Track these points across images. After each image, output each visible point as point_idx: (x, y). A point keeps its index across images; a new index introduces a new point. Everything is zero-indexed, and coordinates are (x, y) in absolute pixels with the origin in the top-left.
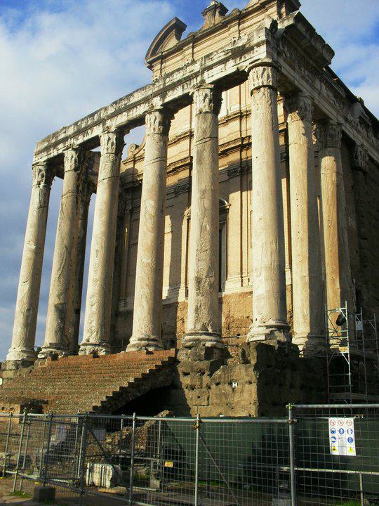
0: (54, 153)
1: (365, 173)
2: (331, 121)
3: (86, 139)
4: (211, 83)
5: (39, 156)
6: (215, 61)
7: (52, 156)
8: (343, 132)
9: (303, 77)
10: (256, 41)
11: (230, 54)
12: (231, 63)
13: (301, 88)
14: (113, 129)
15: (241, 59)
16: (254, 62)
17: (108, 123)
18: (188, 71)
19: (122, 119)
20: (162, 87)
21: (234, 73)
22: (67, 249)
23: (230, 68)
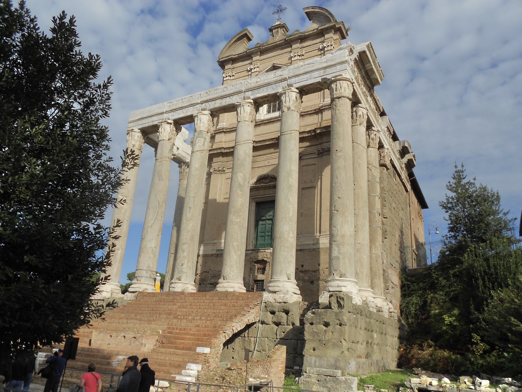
1: (388, 169)
2: (373, 128)
5: (134, 124)
8: (379, 138)
9: (364, 93)
13: (361, 100)
14: (207, 112)
16: (336, 76)
21: (319, 83)
22: (159, 203)
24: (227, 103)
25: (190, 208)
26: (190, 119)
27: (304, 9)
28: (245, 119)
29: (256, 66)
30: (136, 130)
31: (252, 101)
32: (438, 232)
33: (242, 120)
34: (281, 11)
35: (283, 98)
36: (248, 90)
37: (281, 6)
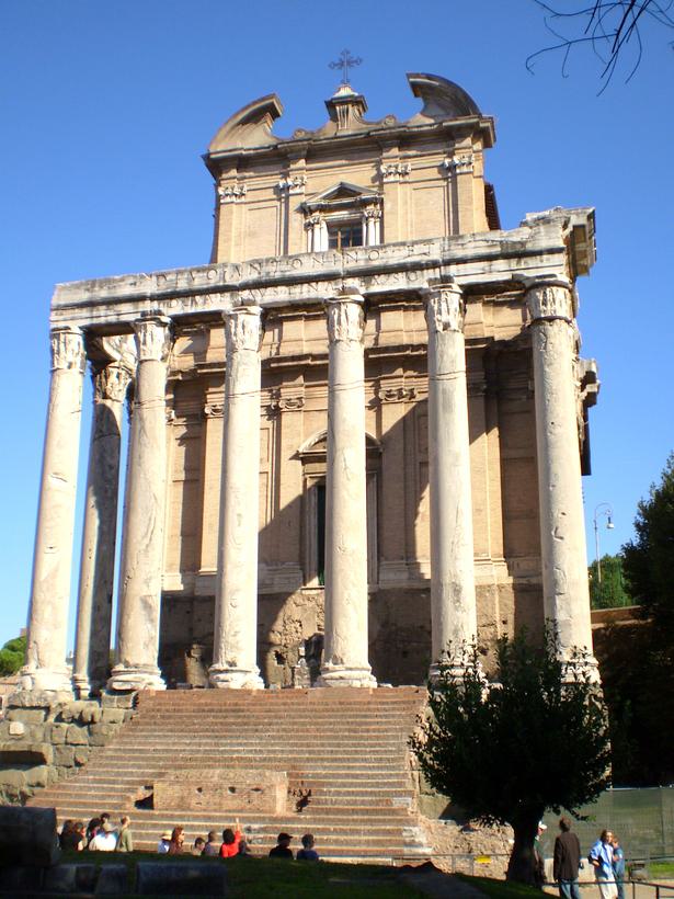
0: (105, 316)
3: (190, 310)
4: (461, 286)
5: (68, 314)
6: (470, 252)
7: (102, 320)
10: (544, 243)
11: (499, 249)
12: (501, 264)
14: (257, 310)
15: (518, 263)
17: (245, 294)
18: (415, 252)
19: (281, 295)
20: (362, 264)
23: (500, 271)
24: (305, 296)
25: (239, 515)
26: (216, 319)
27: (409, 76)
28: (350, 336)
29: (299, 182)
30: (75, 327)
31: (363, 299)
32: (611, 525)
33: (344, 337)
34: (349, 63)
35: (434, 303)
36: (351, 274)
37: (348, 53)
